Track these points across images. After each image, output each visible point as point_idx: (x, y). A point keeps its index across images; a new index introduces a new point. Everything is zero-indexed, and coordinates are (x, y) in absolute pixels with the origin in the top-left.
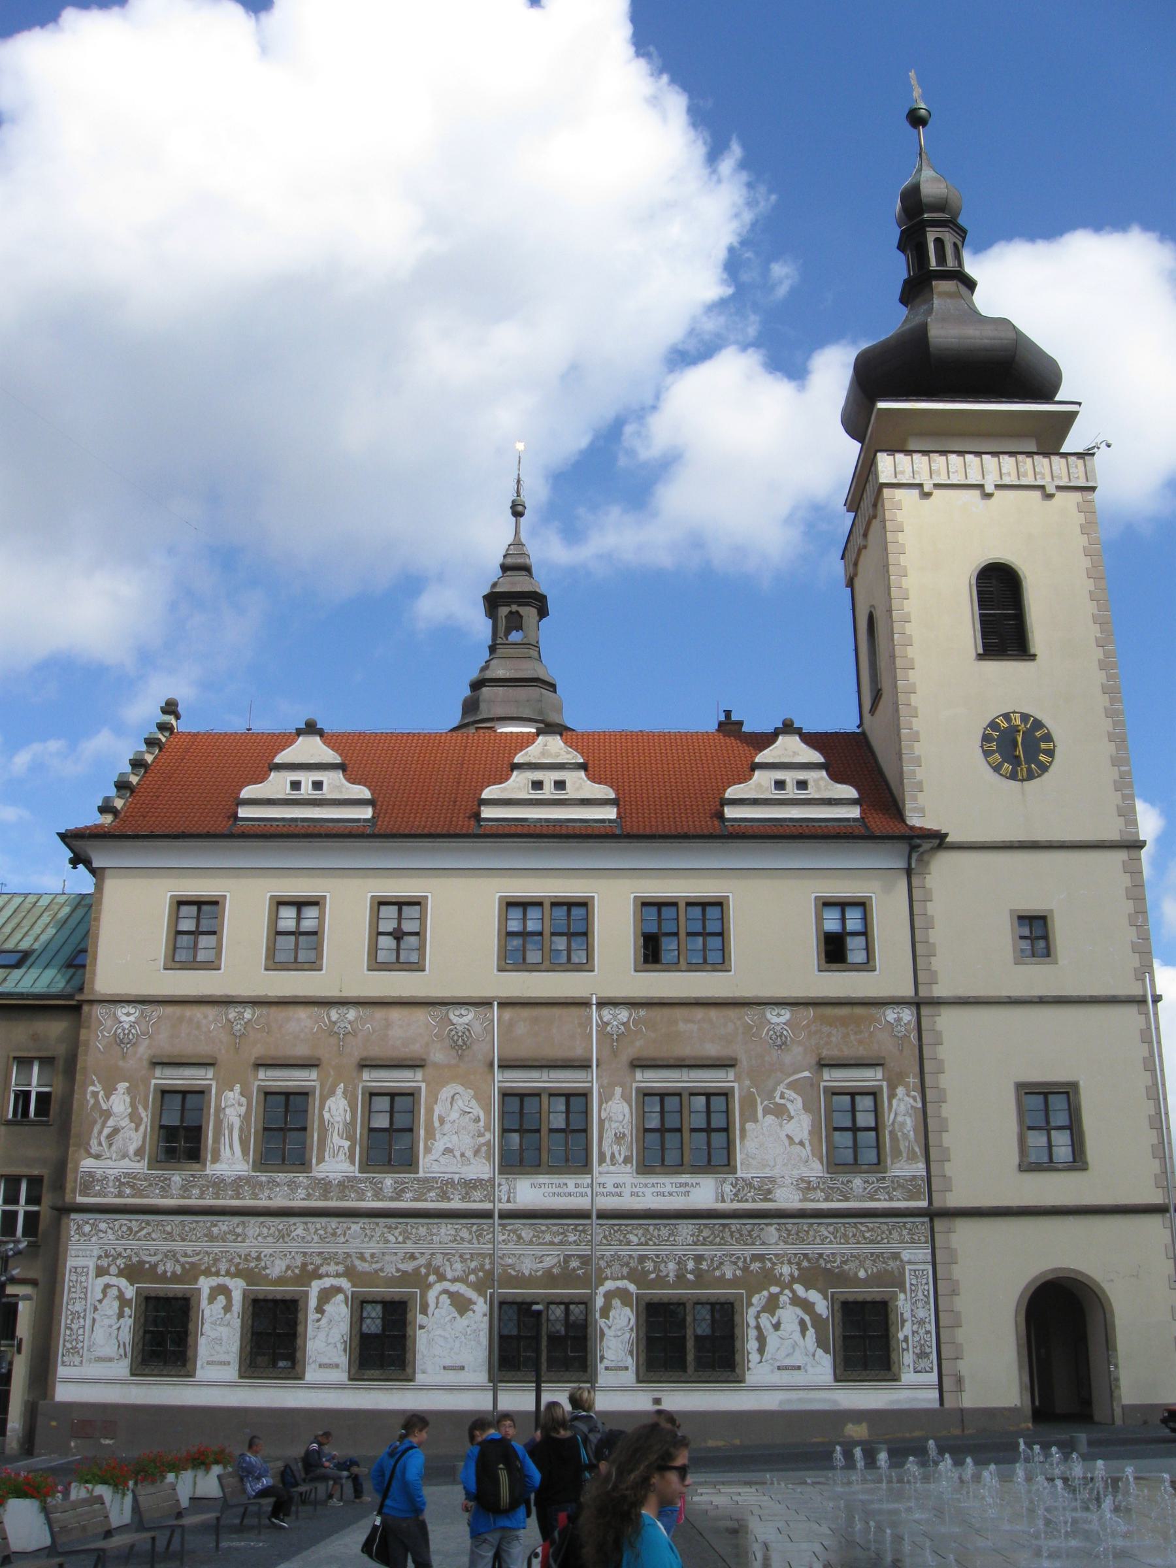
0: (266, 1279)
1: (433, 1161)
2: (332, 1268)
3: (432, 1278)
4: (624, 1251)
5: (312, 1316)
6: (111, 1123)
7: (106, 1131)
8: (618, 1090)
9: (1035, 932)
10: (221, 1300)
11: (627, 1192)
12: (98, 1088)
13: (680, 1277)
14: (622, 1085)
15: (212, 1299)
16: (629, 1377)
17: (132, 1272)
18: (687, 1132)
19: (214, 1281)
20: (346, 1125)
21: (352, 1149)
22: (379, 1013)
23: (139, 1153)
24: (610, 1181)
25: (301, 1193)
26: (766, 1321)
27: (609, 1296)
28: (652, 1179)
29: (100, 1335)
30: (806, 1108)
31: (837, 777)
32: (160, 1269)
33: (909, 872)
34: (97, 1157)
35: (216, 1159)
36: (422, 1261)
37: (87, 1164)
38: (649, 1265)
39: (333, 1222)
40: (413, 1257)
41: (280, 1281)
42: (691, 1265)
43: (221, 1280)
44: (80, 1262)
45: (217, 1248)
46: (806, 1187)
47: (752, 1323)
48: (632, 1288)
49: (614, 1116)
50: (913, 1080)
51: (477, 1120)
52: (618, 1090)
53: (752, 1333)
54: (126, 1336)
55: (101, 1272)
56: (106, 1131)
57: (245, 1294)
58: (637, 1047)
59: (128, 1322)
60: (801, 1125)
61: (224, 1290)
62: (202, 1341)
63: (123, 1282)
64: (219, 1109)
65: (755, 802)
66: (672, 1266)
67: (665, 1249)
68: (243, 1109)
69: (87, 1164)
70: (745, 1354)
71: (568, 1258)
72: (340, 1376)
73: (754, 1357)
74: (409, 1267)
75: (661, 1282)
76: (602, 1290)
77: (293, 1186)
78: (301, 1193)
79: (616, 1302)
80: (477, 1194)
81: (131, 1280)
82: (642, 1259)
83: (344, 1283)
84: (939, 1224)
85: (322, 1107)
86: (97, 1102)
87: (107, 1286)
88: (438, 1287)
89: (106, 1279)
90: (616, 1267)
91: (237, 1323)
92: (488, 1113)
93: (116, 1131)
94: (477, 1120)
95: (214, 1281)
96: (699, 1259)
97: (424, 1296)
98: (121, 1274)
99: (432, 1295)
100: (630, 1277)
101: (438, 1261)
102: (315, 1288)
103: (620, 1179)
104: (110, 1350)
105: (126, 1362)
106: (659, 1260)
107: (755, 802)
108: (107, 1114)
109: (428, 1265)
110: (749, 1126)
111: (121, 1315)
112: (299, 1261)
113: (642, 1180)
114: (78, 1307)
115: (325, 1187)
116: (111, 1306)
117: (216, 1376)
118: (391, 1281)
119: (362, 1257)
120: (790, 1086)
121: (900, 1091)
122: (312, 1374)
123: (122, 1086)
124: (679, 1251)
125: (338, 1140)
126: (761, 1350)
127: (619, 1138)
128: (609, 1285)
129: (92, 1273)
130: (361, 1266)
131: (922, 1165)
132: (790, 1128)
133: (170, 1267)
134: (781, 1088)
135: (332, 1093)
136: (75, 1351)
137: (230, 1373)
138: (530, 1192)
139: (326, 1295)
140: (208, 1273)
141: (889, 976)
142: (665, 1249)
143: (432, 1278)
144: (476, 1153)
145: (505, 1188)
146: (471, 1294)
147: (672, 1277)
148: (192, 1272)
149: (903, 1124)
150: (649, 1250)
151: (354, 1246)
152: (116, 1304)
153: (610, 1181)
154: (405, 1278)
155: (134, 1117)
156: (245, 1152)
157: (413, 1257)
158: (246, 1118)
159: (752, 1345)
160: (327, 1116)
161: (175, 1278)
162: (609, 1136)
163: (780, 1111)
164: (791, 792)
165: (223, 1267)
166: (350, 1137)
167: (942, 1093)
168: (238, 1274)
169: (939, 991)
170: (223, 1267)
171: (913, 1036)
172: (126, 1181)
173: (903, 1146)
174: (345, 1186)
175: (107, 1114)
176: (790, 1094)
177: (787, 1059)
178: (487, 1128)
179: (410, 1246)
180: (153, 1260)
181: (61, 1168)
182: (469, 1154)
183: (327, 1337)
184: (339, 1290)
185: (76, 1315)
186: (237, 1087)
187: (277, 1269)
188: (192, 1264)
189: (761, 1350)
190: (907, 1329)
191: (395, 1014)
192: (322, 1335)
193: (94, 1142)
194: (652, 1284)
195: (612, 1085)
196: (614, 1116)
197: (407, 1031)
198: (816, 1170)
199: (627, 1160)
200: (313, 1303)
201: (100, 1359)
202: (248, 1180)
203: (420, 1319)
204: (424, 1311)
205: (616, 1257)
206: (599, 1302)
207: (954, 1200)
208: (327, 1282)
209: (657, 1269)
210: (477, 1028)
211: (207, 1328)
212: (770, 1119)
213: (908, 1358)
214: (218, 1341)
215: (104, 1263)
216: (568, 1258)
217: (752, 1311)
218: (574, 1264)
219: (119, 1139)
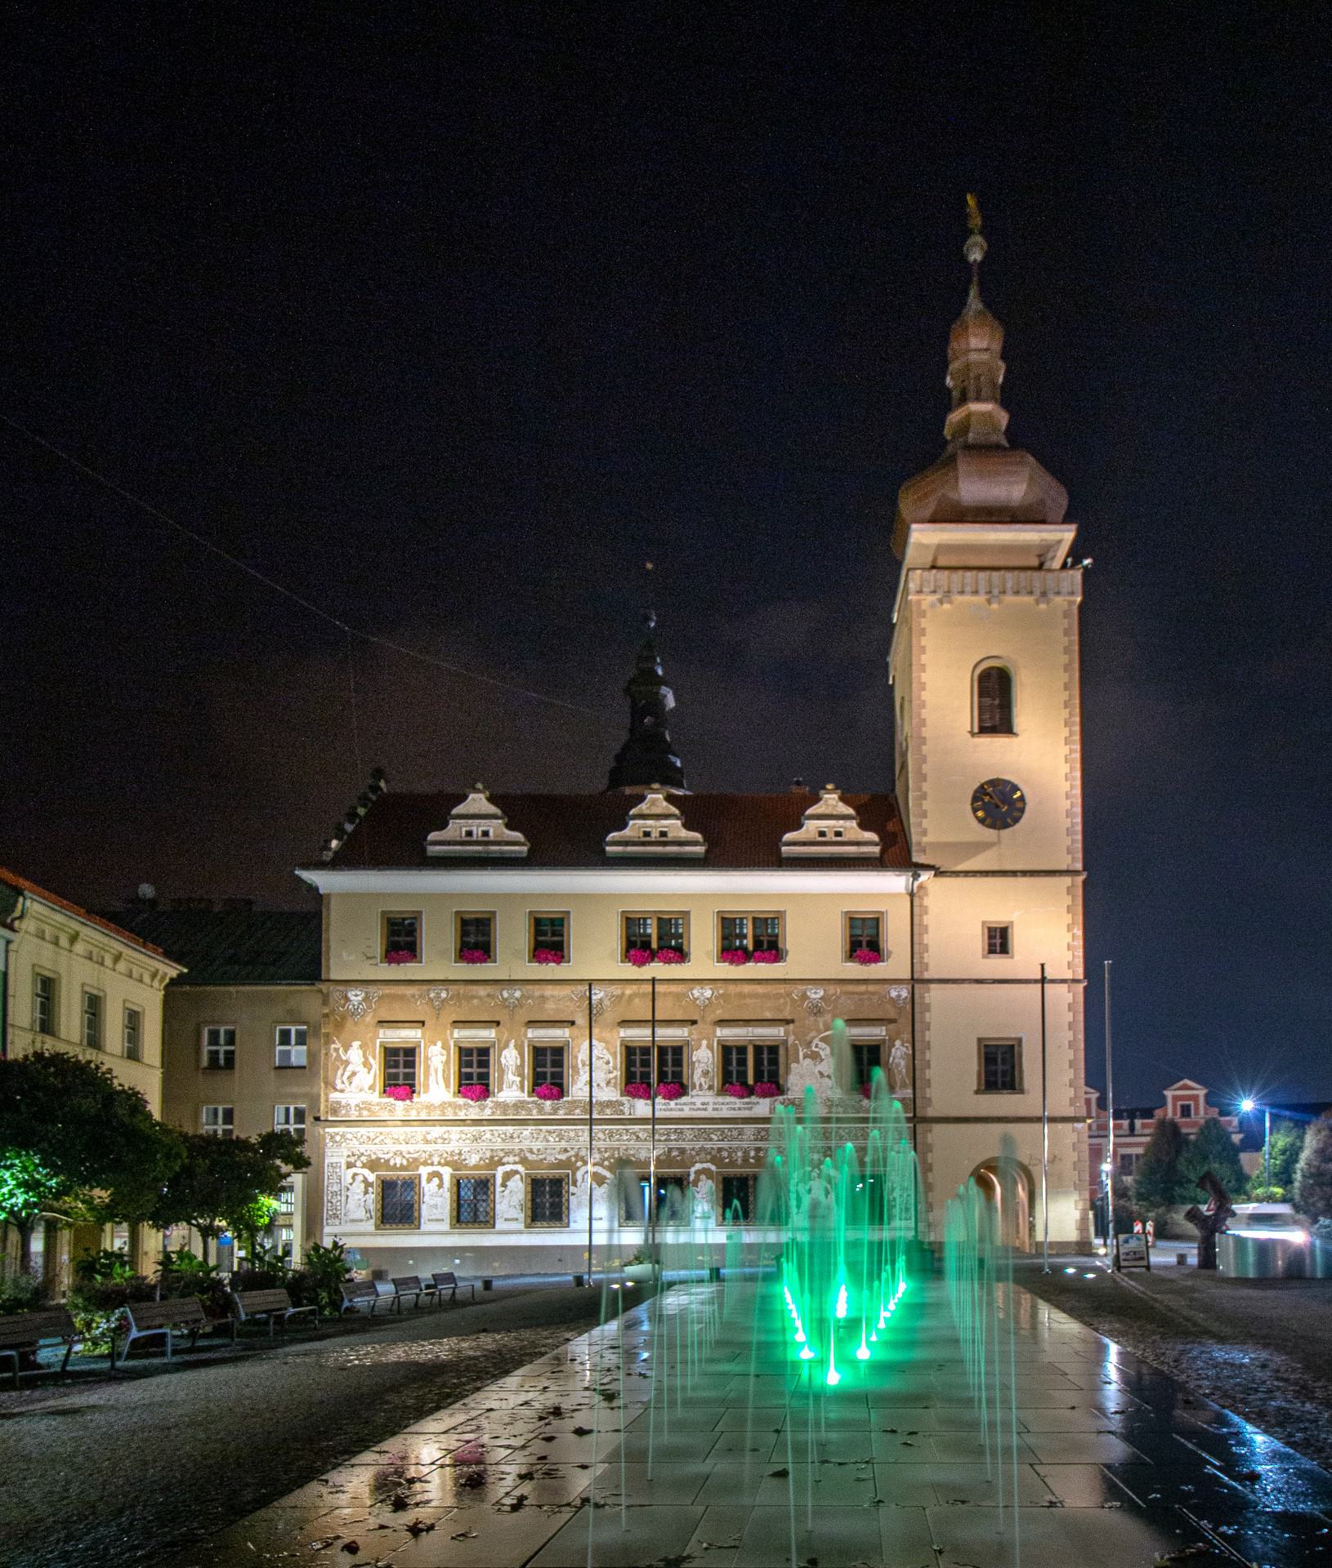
0: (466, 1167)
1: (578, 1089)
2: (511, 1159)
3: (579, 1164)
4: (708, 1145)
5: (499, 1189)
6: (350, 1068)
7: (347, 1074)
8: (704, 1042)
9: (999, 940)
10: (436, 1181)
11: (710, 1108)
12: (338, 1045)
13: (746, 1159)
14: (708, 1039)
15: (429, 1181)
16: (712, 1224)
17: (373, 1165)
18: (754, 1071)
19: (430, 1169)
20: (517, 1067)
21: (522, 1083)
22: (537, 991)
23: (372, 1087)
24: (698, 1101)
25: (488, 1111)
26: (802, 1189)
27: (698, 1173)
28: (729, 1099)
29: (351, 1205)
30: (832, 1054)
31: (863, 826)
32: (392, 1163)
33: (912, 895)
34: (342, 1091)
35: (427, 1090)
36: (572, 1153)
37: (334, 1096)
38: (725, 1154)
39: (510, 1129)
40: (566, 1150)
41: (476, 1167)
42: (752, 1154)
43: (435, 1168)
44: (334, 1160)
45: (430, 1148)
46: (829, 1103)
47: (792, 1188)
48: (713, 1168)
49: (703, 1059)
50: (907, 1036)
51: (608, 1063)
52: (704, 1042)
53: (793, 1196)
54: (372, 1207)
55: (350, 1165)
56: (347, 1074)
57: (452, 1176)
58: (719, 1014)
59: (371, 1197)
60: (828, 1066)
61: (438, 1175)
62: (424, 1207)
63: (366, 1172)
64: (427, 1058)
65: (804, 844)
66: (740, 1154)
67: (735, 1144)
68: (444, 1058)
69: (334, 1096)
70: (787, 1207)
71: (670, 1150)
72: (521, 1226)
73: (794, 1210)
74: (563, 1157)
75: (733, 1164)
76: (693, 1170)
77: (482, 1109)
78: (488, 1111)
79: (703, 1177)
80: (608, 1111)
81: (372, 1170)
82: (720, 1150)
83: (520, 1168)
84: (919, 1127)
85: (500, 1055)
86: (338, 1055)
87: (355, 1175)
88: (583, 1170)
89: (354, 1170)
90: (703, 1155)
91: (448, 1195)
92: (615, 1058)
93: (354, 1074)
94: (608, 1063)
95: (430, 1169)
96: (758, 1150)
97: (574, 1174)
98: (364, 1166)
99: (579, 1175)
100: (712, 1161)
101: (583, 1153)
102: (500, 1172)
103: (706, 1100)
104: (361, 1214)
105: (372, 1221)
106: (731, 1151)
107: (804, 844)
108: (347, 1063)
109: (576, 1155)
110: (794, 1065)
111: (366, 1192)
112: (488, 1155)
113: (720, 1099)
114: (336, 1188)
115: (504, 1106)
116: (359, 1187)
117: (436, 1225)
118: (552, 1166)
119: (531, 1151)
120: (822, 1040)
121: (898, 1043)
122: (500, 1225)
123: (356, 1044)
124: (745, 1145)
125: (511, 1077)
126: (798, 1207)
127: (706, 1073)
128: (698, 1166)
129: (344, 1166)
130: (530, 1157)
131: (910, 1091)
132: (820, 1068)
133: (398, 1161)
134: (816, 1041)
135: (506, 1046)
136: (336, 1216)
137: (445, 1226)
138: (642, 1108)
139: (508, 1176)
140: (425, 1164)
141: (895, 965)
142: (735, 1144)
143: (579, 1164)
144: (608, 1083)
145: (627, 1105)
146: (607, 1174)
147: (740, 1161)
148: (414, 1163)
149: (898, 1065)
150: (724, 1144)
151: (525, 1145)
152: (363, 1186)
153: (698, 1101)
154: (560, 1164)
155: (366, 1064)
156: (447, 1086)
157: (566, 1150)
158: (447, 1063)
159: (793, 1203)
160: (503, 1061)
161: (403, 1168)
162: (698, 1073)
163: (815, 1056)
164: (831, 837)
165: (436, 1159)
166: (521, 1075)
167: (928, 1045)
168: (447, 1164)
169: (926, 976)
170: (436, 1159)
171: (909, 1007)
172: (367, 1106)
173: (898, 1078)
174: (519, 1106)
175: (347, 1063)
176: (822, 1045)
177: (821, 1020)
178: (615, 1068)
179: (563, 1144)
180: (387, 1157)
181: (315, 1100)
182: (603, 1084)
183: (510, 1200)
184: (517, 1172)
185: (334, 1194)
186: (439, 1044)
187: (473, 1160)
188: (415, 1160)
189: (798, 1207)
190: (897, 1194)
191: (549, 991)
192: (505, 1202)
193: (338, 1082)
194: (727, 1166)
195: (700, 1040)
196: (703, 1059)
197: (558, 1001)
198: (837, 1094)
199: (710, 1088)
200: (499, 1181)
201: (353, 1221)
202: (450, 1104)
203: (572, 1189)
204: (575, 1184)
205: (702, 1149)
206: (692, 1178)
207: (931, 1112)
208: (508, 1168)
209: (730, 1156)
210: (607, 1002)
211: (426, 1199)
212: (808, 1061)
213: (896, 1211)
214: (436, 1206)
215: (352, 1159)
216: (670, 1150)
217: (793, 1182)
218: (674, 1153)
219: (355, 1080)
